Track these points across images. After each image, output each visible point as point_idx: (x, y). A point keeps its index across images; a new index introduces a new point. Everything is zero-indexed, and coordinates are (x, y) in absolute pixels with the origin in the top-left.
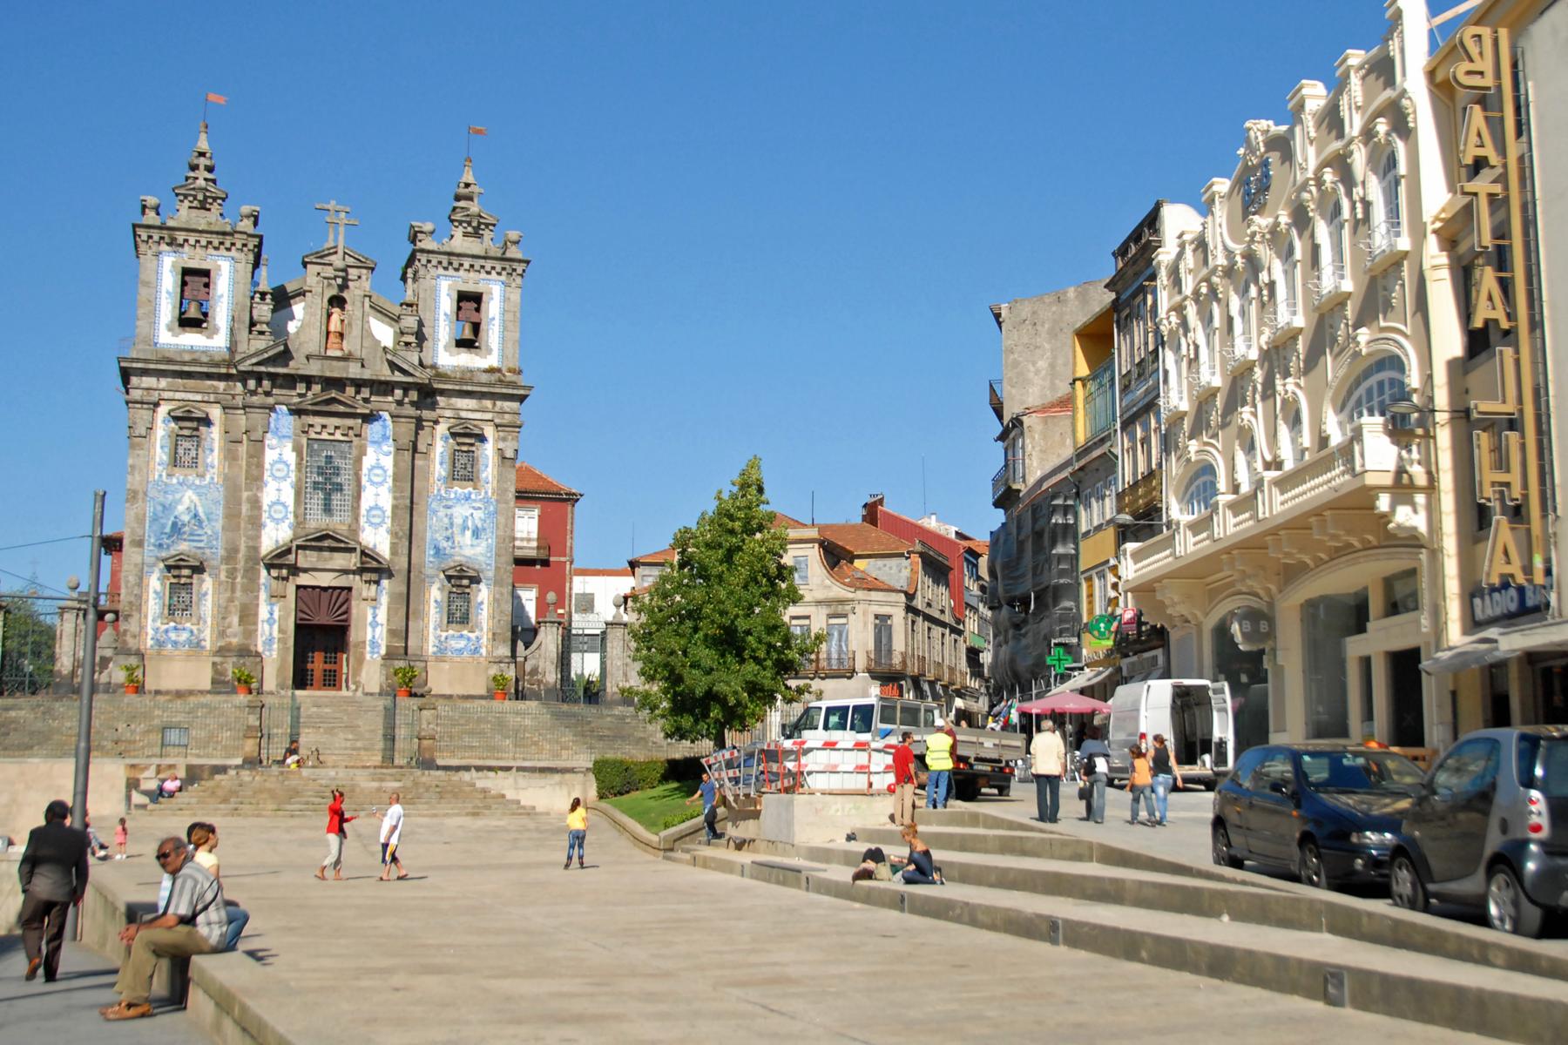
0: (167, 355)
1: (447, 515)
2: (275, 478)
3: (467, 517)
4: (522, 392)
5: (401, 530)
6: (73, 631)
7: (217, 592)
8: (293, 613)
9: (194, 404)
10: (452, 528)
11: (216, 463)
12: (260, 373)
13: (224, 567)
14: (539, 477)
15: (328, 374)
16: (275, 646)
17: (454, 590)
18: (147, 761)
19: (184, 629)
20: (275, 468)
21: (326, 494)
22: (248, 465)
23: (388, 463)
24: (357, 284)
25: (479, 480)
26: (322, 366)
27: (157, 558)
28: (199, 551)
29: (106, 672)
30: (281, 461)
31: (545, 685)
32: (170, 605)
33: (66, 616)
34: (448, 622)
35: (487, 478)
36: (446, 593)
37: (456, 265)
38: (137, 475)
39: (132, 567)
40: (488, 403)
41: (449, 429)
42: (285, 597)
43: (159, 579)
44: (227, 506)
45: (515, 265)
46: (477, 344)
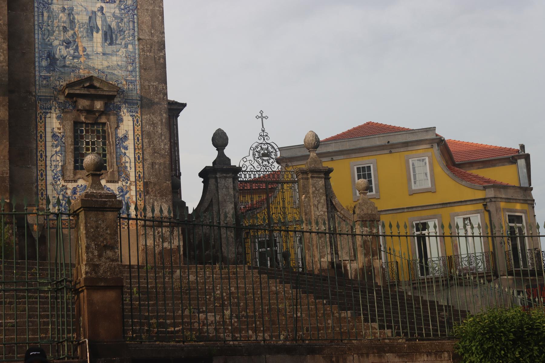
1: (64, 10)
3: (94, 13)
10: (73, 29)
17: (83, 119)
34: (76, 168)
36: (69, 125)
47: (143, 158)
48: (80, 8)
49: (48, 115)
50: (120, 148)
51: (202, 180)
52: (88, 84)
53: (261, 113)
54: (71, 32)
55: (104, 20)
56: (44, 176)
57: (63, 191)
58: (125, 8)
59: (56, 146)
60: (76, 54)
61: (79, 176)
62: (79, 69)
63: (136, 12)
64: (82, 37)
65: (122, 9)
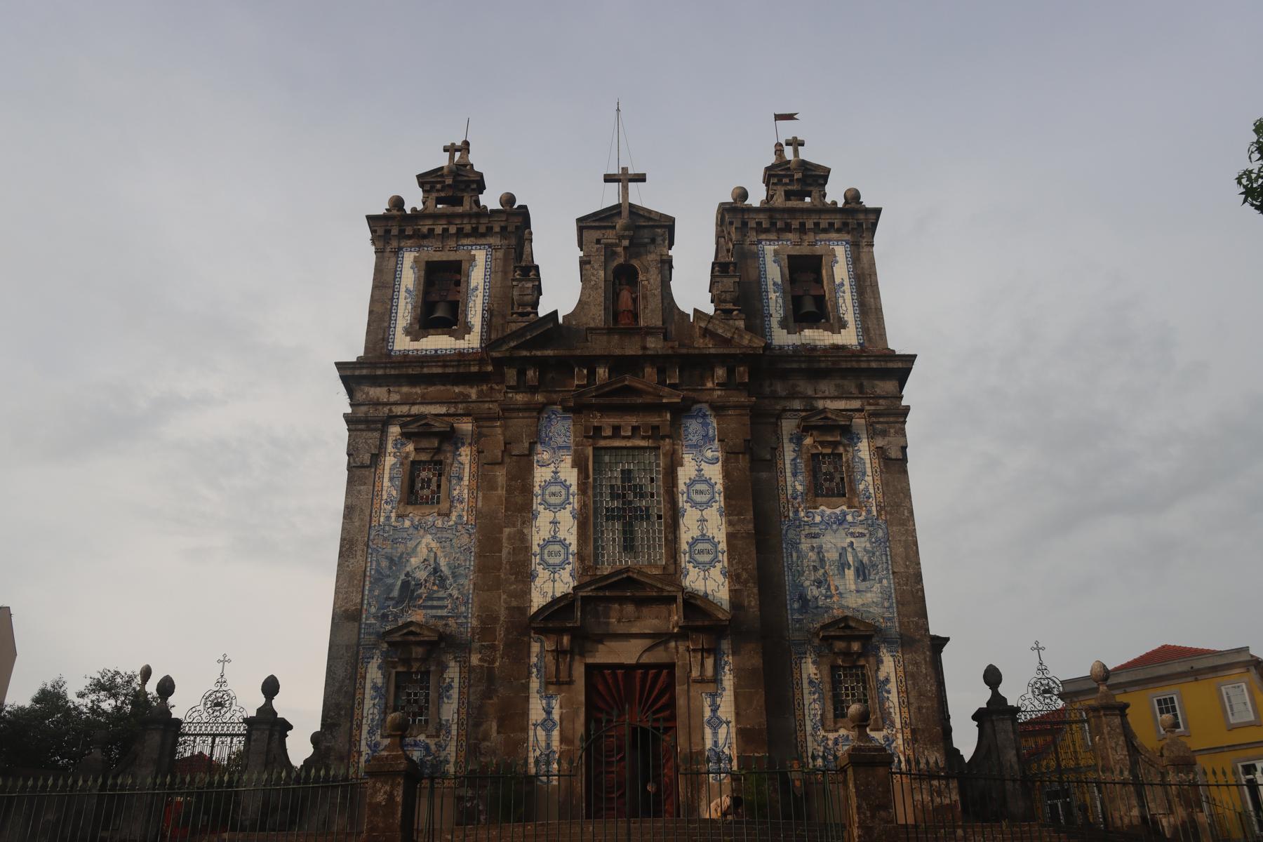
2: (548, 506)
3: (844, 549)
4: (900, 365)
5: (746, 570)
7: (466, 684)
8: (584, 709)
15: (618, 352)
17: (840, 662)
19: (416, 744)
20: (547, 492)
21: (624, 525)
22: (510, 490)
23: (715, 473)
30: (556, 480)
33: (255, 735)
34: (836, 716)
35: (867, 488)
36: (826, 669)
40: (851, 385)
41: (798, 427)
43: (379, 667)
44: (479, 556)
45: (861, 216)
46: (823, 321)
47: (908, 702)
49: (804, 661)
50: (882, 692)
51: (976, 723)
52: (843, 625)
53: (1037, 643)
54: (822, 571)
55: (855, 555)
56: (803, 727)
57: (823, 742)
58: (876, 541)
60: (829, 593)
61: (839, 725)
62: (833, 609)
63: (887, 544)
64: (833, 575)
65: (874, 543)
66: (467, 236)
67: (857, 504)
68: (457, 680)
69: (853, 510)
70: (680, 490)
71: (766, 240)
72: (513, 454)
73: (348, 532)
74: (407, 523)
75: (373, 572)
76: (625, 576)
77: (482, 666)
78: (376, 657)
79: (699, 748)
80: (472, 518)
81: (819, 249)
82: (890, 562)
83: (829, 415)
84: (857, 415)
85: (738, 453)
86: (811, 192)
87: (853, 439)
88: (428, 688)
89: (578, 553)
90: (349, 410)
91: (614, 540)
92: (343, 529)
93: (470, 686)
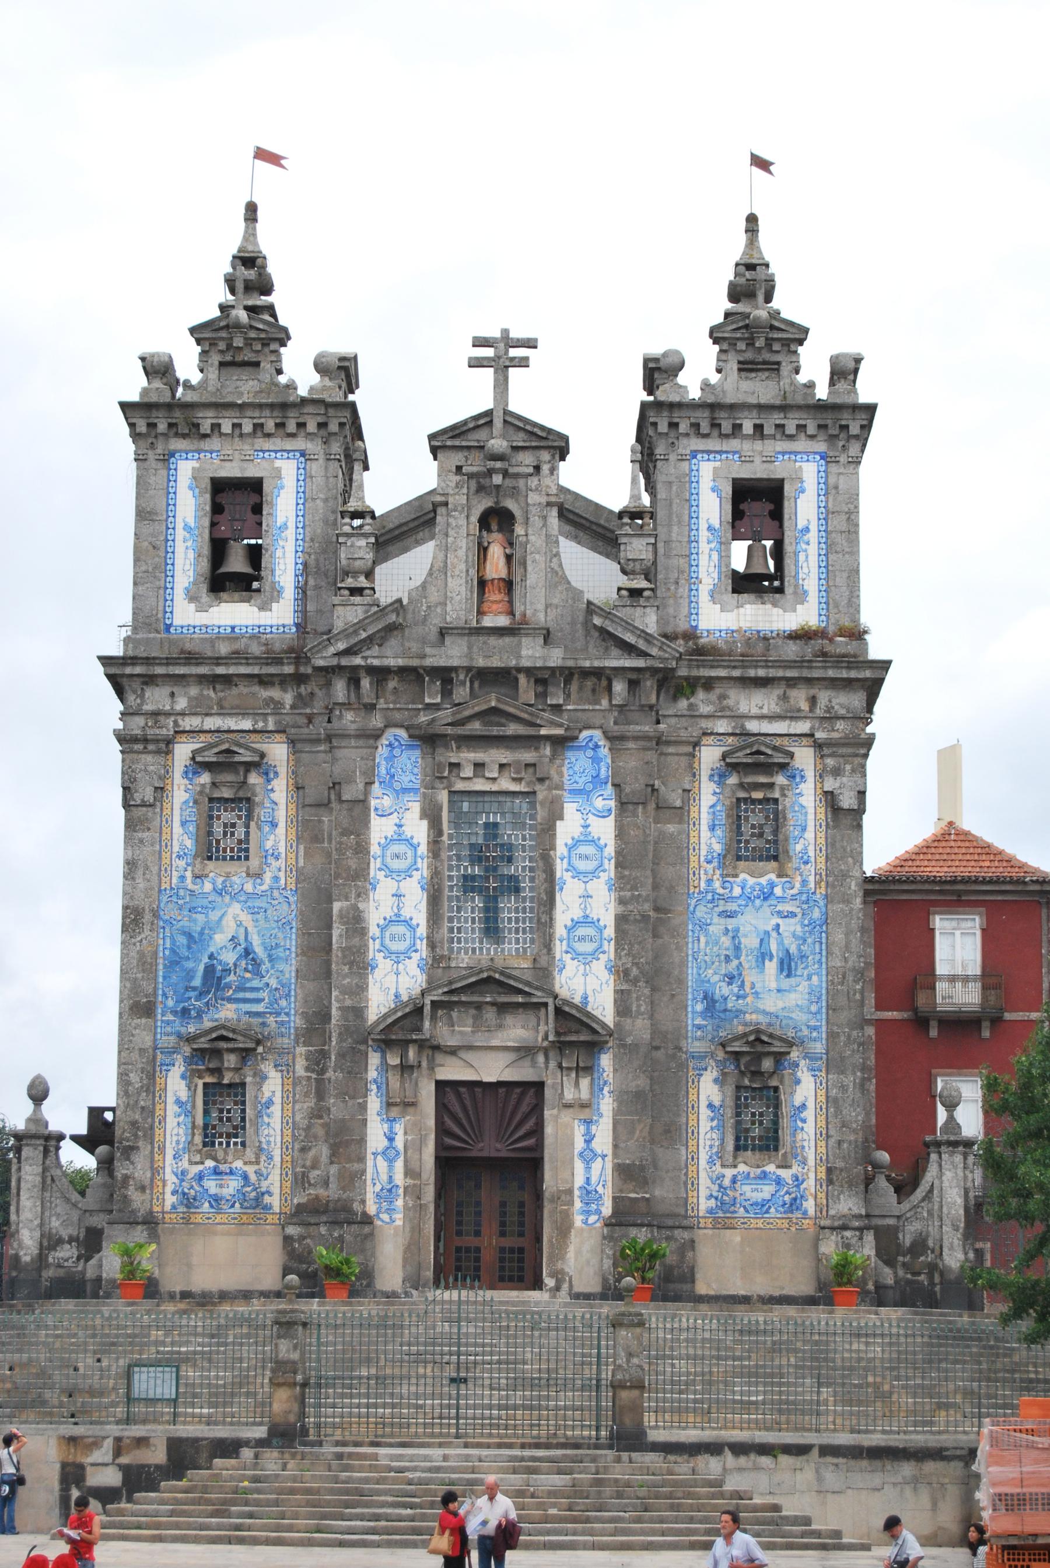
0: (188, 646)
2: (390, 872)
3: (767, 933)
4: (868, 674)
5: (637, 964)
6: (39, 1179)
8: (433, 1136)
9: (239, 736)
10: (738, 957)
11: (282, 850)
12: (355, 668)
13: (301, 1050)
14: (987, 850)
15: (481, 662)
16: (400, 1203)
17: (747, 1082)
18: (96, 1430)
19: (231, 1173)
20: (389, 853)
23: (605, 830)
24: (533, 482)
25: (790, 858)
26: (470, 647)
27: (179, 1036)
28: (256, 1021)
29: (97, 1257)
30: (399, 838)
31: (942, 1274)
32: (206, 1126)
33: (26, 1152)
34: (737, 1148)
36: (730, 1090)
37: (726, 427)
38: (139, 880)
39: (135, 1056)
40: (799, 697)
41: (724, 757)
42: (413, 1104)
43: (183, 1077)
44: (304, 933)
45: (845, 418)
48: (748, 928)
49: (702, 1079)
52: (752, 1038)
54: (735, 962)
55: (780, 943)
59: (712, 1120)
61: (740, 1159)
64: (750, 968)
66: (268, 435)
67: (789, 873)
68: (278, 1094)
69: (784, 880)
70: (558, 854)
71: (703, 452)
72: (345, 797)
73: (132, 898)
74: (208, 887)
75: (167, 952)
76: (485, 975)
77: (309, 1078)
78: (177, 1064)
79: (568, 1186)
80: (292, 881)
81: (778, 470)
82: (824, 953)
83: (763, 749)
84: (805, 741)
85: (638, 804)
86: (778, 363)
87: (794, 777)
88: (244, 1103)
89: (428, 938)
90: (120, 725)
91: (473, 919)
92: (125, 893)
93: (295, 1102)
